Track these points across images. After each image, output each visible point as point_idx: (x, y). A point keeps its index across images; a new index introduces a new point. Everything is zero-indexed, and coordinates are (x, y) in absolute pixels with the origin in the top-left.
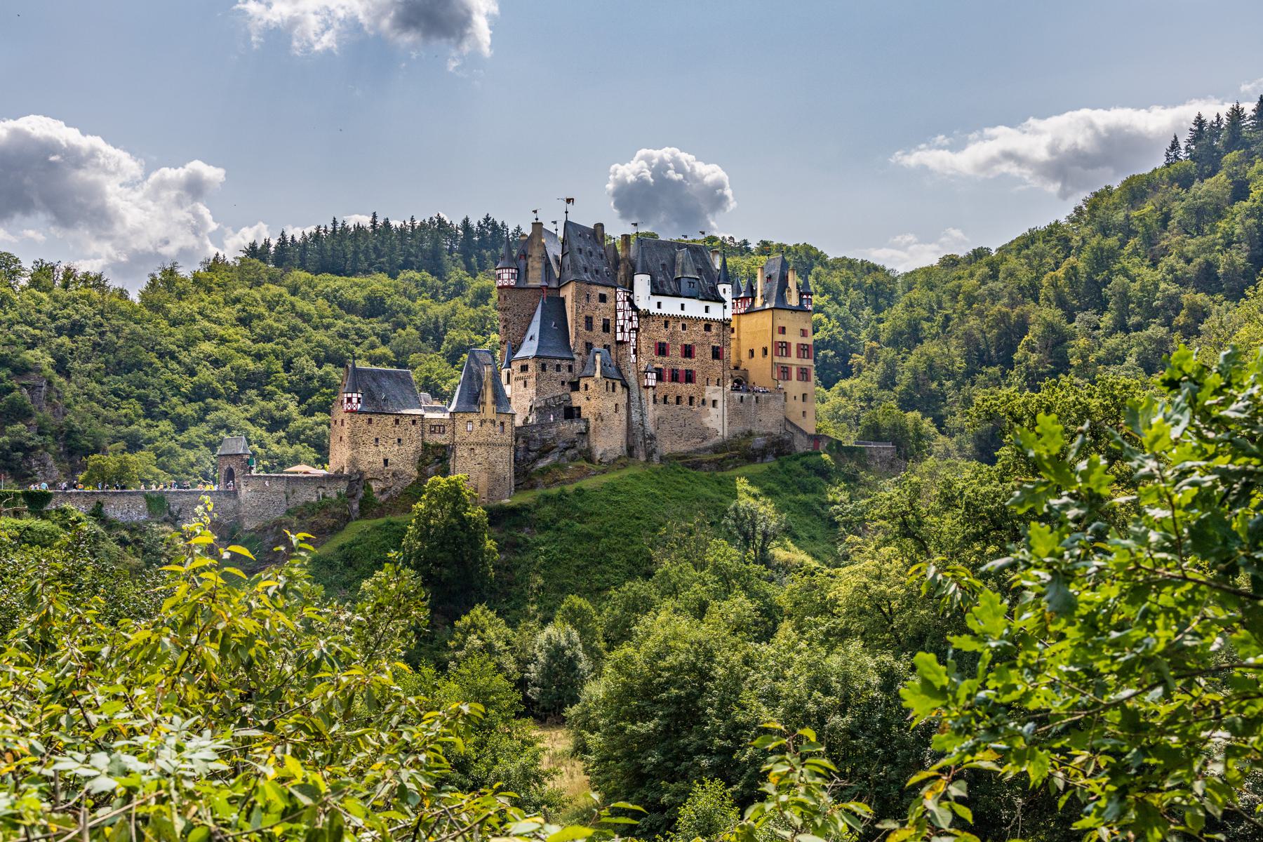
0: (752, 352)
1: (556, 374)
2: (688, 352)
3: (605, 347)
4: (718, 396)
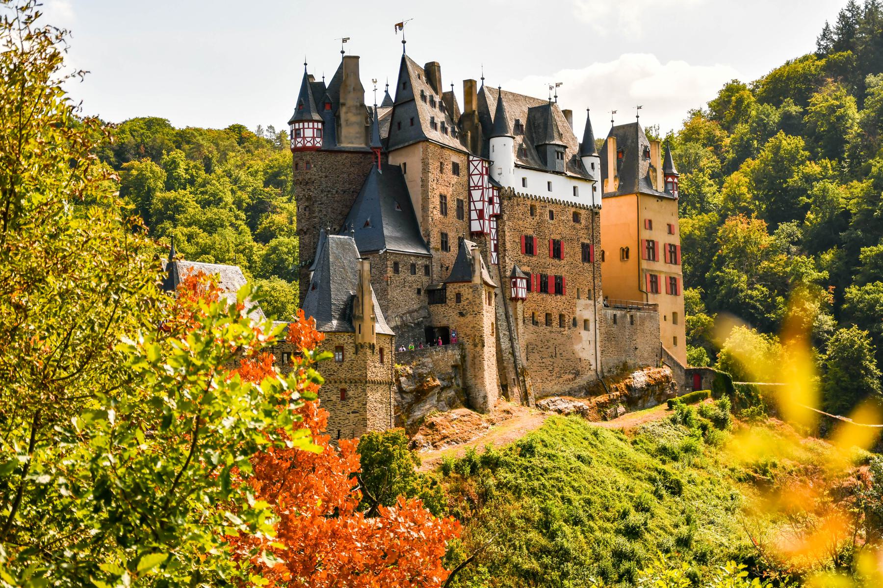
1: (411, 278)
2: (557, 251)
4: (588, 314)
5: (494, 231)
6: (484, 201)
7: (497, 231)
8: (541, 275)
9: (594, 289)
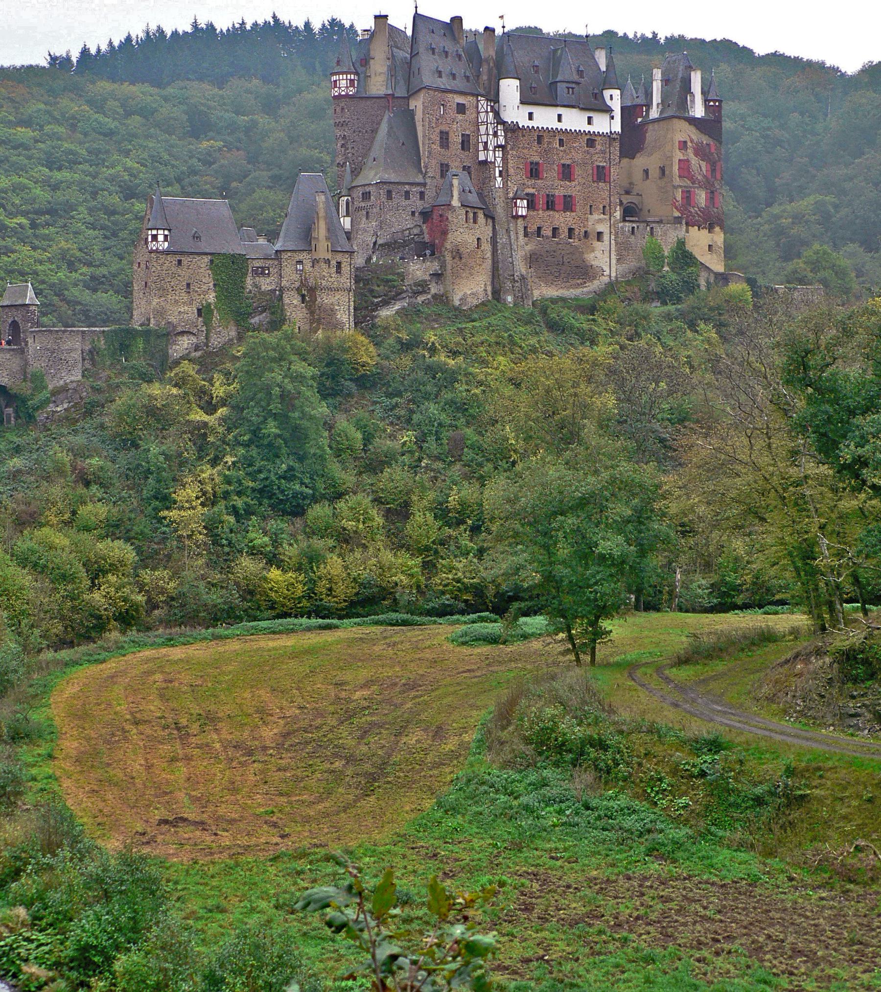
0: (646, 172)
1: (405, 203)
2: (567, 172)
3: (464, 168)
4: (603, 228)
5: (499, 160)
6: (488, 135)
7: (503, 159)
8: (548, 195)
9: (610, 205)
